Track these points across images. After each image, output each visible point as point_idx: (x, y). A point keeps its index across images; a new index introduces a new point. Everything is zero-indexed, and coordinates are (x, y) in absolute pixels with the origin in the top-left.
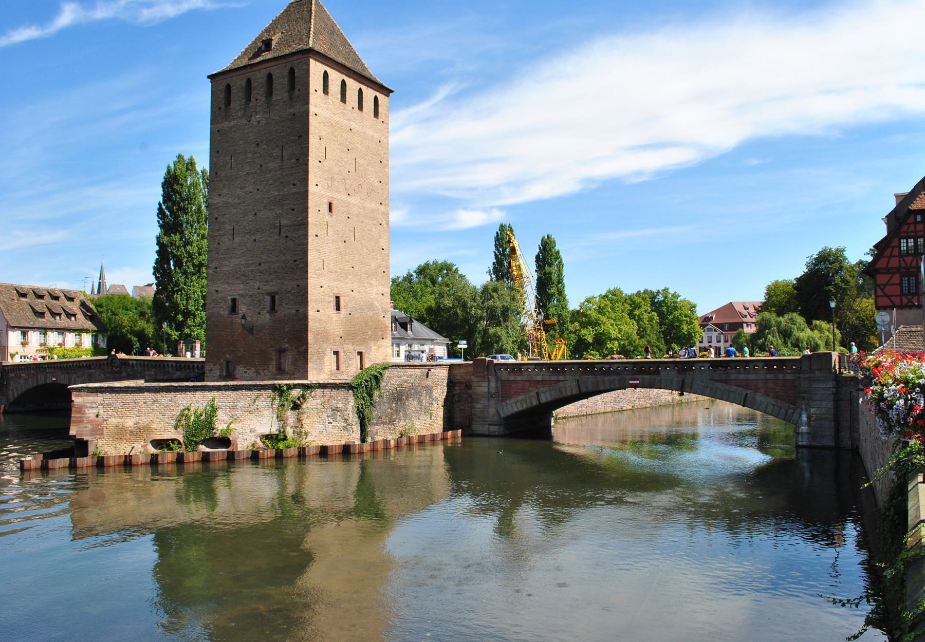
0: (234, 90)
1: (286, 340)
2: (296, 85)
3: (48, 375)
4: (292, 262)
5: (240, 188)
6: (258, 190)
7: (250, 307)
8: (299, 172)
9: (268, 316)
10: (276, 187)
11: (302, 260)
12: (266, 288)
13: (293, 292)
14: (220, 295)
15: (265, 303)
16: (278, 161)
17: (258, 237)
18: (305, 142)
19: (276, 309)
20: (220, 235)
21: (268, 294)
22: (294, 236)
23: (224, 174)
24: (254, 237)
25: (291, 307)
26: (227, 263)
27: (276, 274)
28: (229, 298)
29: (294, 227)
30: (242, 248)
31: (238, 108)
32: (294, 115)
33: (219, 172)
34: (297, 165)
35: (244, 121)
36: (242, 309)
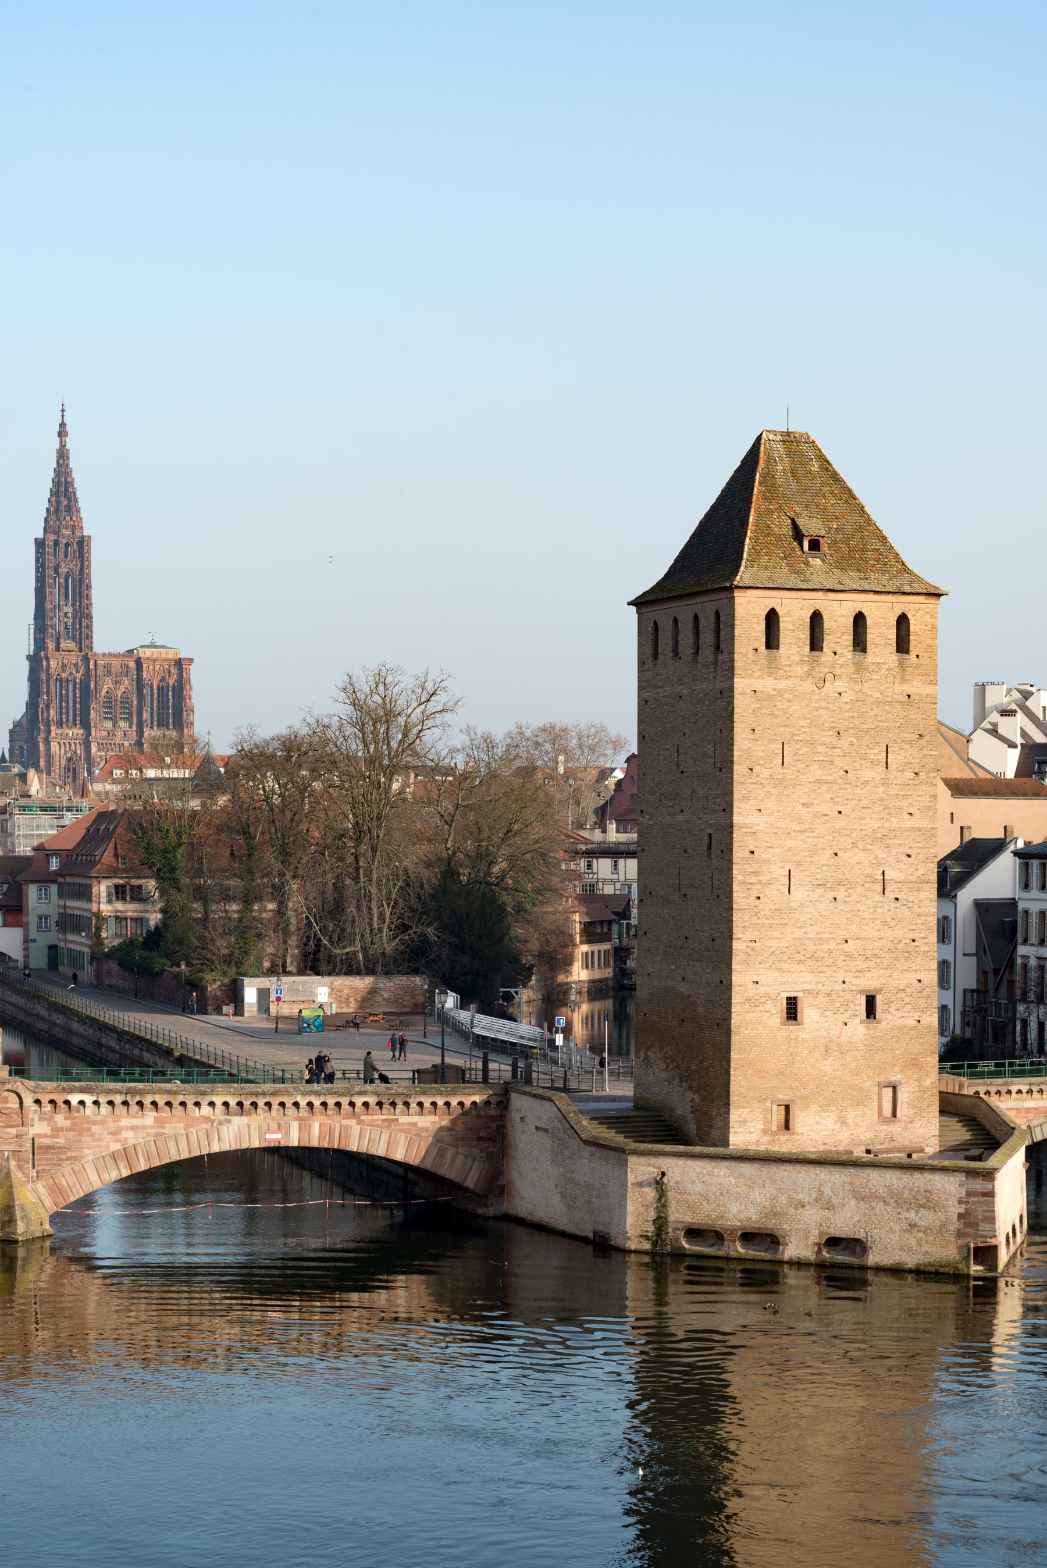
1: (897, 1069)
2: (911, 648)
4: (907, 941)
5: (804, 804)
6: (840, 812)
7: (827, 1013)
8: (918, 796)
10: (875, 813)
11: (926, 941)
12: (858, 981)
14: (762, 990)
15: (858, 1008)
16: (882, 767)
17: (841, 894)
18: (930, 747)
21: (861, 992)
22: (910, 899)
23: (767, 773)
25: (905, 1015)
26: (776, 934)
27: (878, 960)
28: (784, 995)
29: (911, 885)
30: (809, 911)
31: (797, 658)
32: (909, 696)
34: (917, 782)
35: (809, 686)
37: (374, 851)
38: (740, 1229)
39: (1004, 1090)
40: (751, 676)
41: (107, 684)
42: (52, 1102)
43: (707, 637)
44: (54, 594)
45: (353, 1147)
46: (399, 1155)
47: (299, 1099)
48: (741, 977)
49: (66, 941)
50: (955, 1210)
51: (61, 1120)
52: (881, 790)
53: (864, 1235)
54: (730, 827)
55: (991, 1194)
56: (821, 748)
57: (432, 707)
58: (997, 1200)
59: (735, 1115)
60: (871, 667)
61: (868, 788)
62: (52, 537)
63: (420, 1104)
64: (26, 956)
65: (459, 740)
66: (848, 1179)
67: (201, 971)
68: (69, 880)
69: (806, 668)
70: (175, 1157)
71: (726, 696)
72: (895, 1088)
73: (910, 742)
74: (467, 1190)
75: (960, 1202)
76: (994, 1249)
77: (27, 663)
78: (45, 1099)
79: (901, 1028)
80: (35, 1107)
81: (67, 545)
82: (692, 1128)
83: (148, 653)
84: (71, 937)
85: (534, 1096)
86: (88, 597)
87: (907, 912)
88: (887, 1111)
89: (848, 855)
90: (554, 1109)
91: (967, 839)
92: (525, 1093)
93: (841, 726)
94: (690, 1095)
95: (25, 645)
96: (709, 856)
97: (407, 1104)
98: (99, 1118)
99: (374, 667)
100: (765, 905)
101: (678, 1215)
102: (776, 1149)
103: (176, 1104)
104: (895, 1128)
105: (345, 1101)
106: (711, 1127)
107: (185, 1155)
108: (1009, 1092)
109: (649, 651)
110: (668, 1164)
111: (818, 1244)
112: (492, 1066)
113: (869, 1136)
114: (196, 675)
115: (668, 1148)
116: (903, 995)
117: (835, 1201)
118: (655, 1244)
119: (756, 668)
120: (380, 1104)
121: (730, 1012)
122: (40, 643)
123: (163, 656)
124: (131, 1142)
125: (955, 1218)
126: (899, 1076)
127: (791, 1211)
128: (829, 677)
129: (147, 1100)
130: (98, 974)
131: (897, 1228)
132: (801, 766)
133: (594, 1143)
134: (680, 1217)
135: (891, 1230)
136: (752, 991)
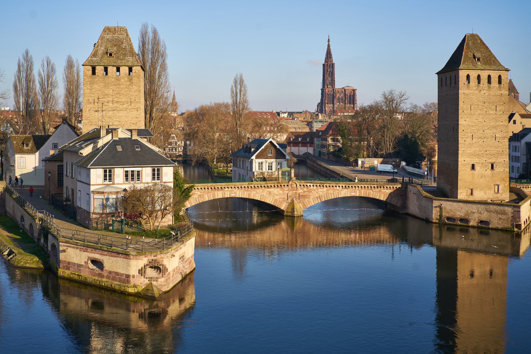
0: (471, 78)
1: (499, 181)
3: (226, 192)
9: (490, 172)
13: (502, 163)
14: (466, 162)
16: (495, 111)
19: (494, 168)
20: (465, 137)
21: (490, 163)
23: (467, 112)
24: (483, 140)
26: (469, 149)
28: (471, 164)
31: (474, 85)
33: (464, 111)
35: (477, 92)
36: (477, 167)
37: (388, 130)
38: (459, 218)
39: (527, 187)
40: (463, 90)
41: (338, 95)
42: (303, 185)
43: (453, 81)
44: (327, 76)
45: (371, 197)
46: (382, 199)
47: (359, 185)
48: (461, 159)
49: (322, 150)
50: (511, 215)
51: (305, 189)
52: (495, 116)
53: (488, 220)
54: (458, 124)
55: (520, 212)
56: (480, 106)
57: (402, 99)
58: (521, 213)
59: (459, 191)
60: (492, 87)
61: (492, 115)
62: (326, 63)
63: (387, 187)
64: (314, 153)
65: (409, 106)
66: (485, 207)
67: (349, 157)
68: (323, 137)
69: (476, 88)
70: (331, 198)
71: (457, 94)
72: (498, 186)
73: (502, 105)
74: (398, 207)
75: (512, 213)
76: (520, 225)
77: (321, 91)
78: (302, 185)
79: (500, 172)
80: (300, 186)
81: (330, 65)
82: (450, 194)
83: (347, 88)
84: (323, 149)
85: (413, 186)
86: (334, 76)
87: (501, 144)
88: (496, 191)
89: (487, 131)
90: (417, 189)
91: (524, 128)
92: (411, 185)
93: (485, 101)
94: (449, 186)
95: (320, 87)
96: (453, 131)
97: (384, 187)
98: (314, 189)
99: (390, 90)
100: (467, 143)
101: (444, 214)
102: (469, 199)
103: (331, 186)
104: (498, 195)
105: (369, 186)
106: (453, 194)
107: (333, 198)
108: (528, 187)
109: (440, 84)
110: (442, 202)
111: (478, 222)
112: (405, 179)
113: (492, 197)
114: (357, 92)
115: (443, 199)
116: (500, 164)
117: (482, 212)
118: (439, 221)
119: (464, 88)
120: (377, 187)
121: (458, 167)
122: (324, 86)
123: (350, 89)
124: (321, 195)
125: (511, 217)
126: (499, 183)
127: (471, 214)
128: (482, 90)
129: (325, 185)
130: (328, 157)
131: (497, 219)
132: (475, 110)
133: (426, 197)
134: (445, 215)
135: (495, 219)
136: (463, 162)
